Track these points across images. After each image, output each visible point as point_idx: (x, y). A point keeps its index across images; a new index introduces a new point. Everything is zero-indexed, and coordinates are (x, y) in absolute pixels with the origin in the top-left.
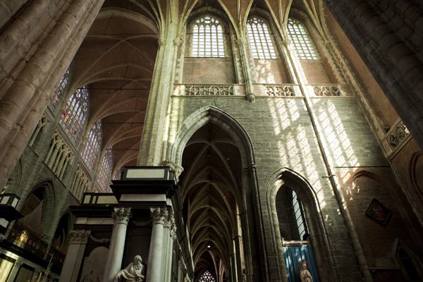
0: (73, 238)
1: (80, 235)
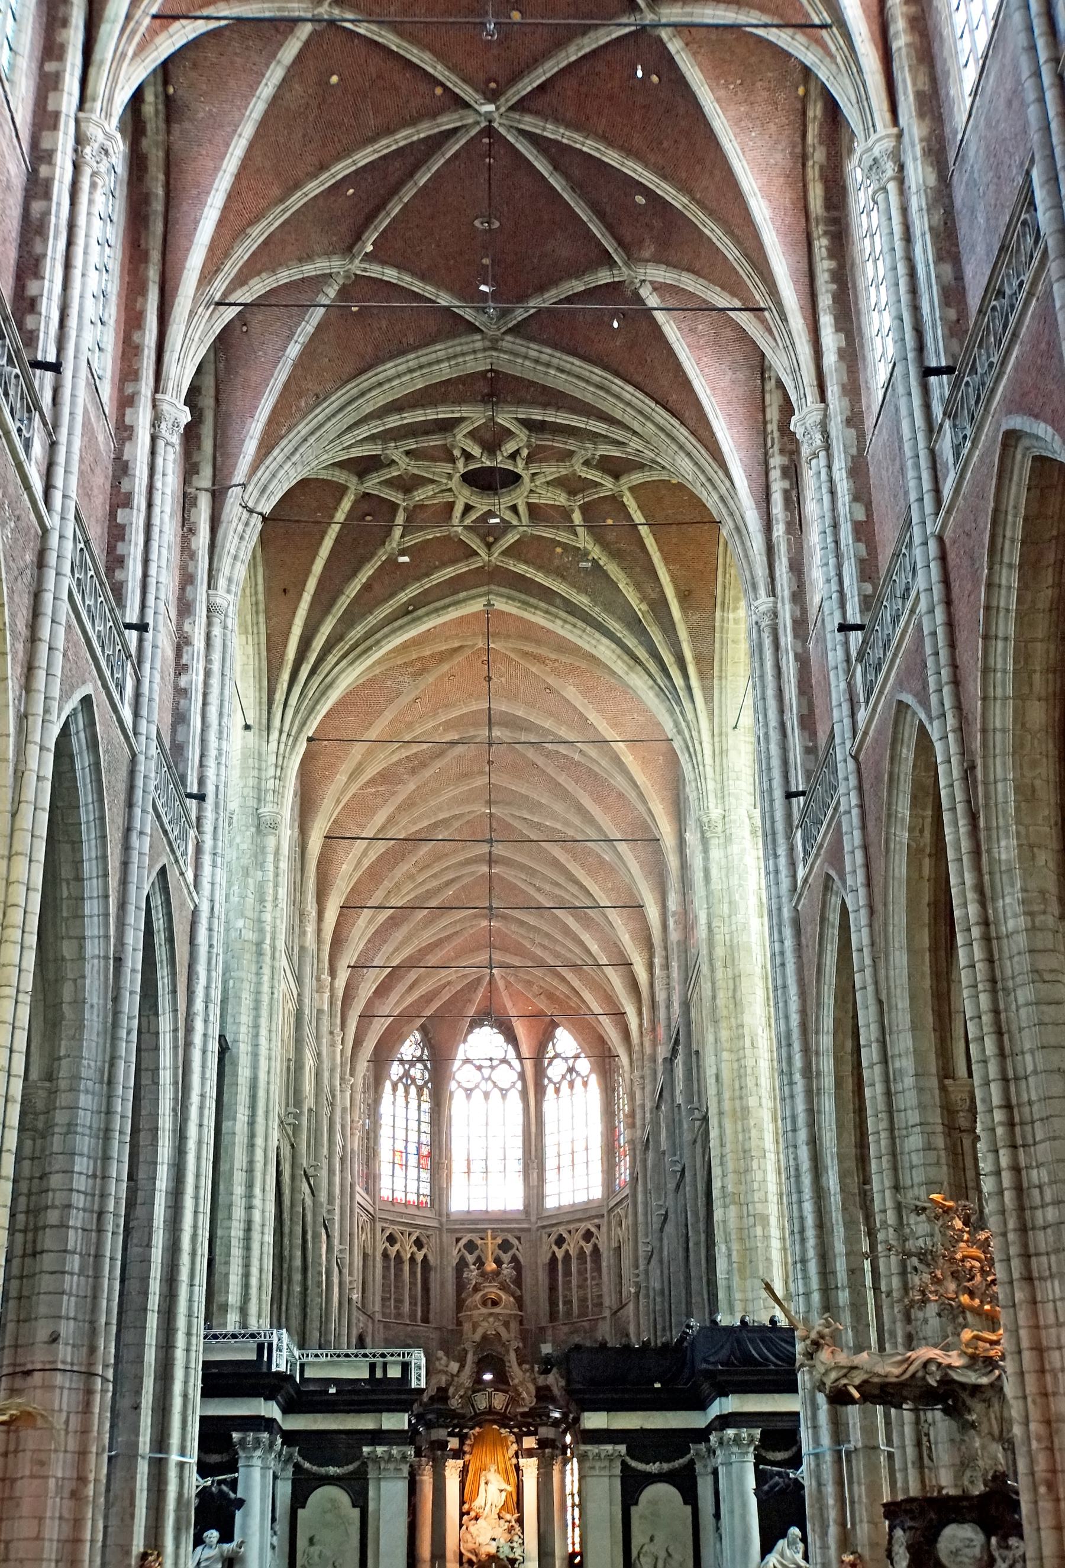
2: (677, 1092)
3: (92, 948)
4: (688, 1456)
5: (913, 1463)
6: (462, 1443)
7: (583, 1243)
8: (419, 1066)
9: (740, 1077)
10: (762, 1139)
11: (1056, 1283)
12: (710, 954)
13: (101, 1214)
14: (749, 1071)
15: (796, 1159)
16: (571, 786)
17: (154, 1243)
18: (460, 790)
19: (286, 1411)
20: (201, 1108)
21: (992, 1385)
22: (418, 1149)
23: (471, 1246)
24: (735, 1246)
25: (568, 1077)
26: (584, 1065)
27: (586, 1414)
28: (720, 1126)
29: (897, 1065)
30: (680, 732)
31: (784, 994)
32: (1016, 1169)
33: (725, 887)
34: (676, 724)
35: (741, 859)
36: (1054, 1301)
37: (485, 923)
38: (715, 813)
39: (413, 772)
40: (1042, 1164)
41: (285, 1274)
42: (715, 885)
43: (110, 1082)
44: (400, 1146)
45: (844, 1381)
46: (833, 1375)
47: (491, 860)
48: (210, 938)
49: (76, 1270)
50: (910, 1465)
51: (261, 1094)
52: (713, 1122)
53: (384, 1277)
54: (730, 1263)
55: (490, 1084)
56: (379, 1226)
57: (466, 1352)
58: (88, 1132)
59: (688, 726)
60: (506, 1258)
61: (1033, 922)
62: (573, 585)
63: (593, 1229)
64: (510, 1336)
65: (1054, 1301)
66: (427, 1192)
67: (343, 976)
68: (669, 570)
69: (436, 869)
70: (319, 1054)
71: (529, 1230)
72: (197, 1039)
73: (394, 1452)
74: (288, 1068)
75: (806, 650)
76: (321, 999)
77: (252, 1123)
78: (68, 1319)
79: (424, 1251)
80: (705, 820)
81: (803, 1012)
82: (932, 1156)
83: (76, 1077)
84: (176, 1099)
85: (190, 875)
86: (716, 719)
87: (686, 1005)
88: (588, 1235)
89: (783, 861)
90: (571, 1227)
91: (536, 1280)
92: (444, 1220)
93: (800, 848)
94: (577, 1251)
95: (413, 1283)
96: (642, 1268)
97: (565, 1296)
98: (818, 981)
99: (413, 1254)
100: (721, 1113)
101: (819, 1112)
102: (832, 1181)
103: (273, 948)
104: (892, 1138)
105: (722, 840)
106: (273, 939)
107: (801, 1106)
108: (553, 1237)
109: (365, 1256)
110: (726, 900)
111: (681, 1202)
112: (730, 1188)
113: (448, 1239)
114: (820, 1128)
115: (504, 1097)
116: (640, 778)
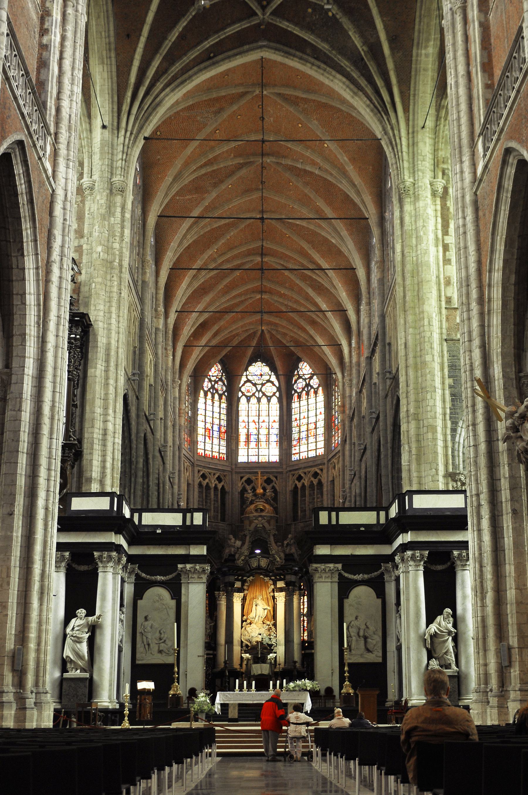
0: (317, 575)
1: (327, 570)
2: (375, 376)
7: (312, 479)
9: (420, 344)
10: (434, 380)
14: (427, 339)
15: (471, 359)
23: (249, 481)
25: (306, 389)
26: (315, 382)
28: (407, 375)
30: (386, 133)
31: (465, 252)
33: (414, 228)
34: (384, 129)
35: (425, 210)
53: (199, 497)
55: (261, 394)
56: (196, 469)
59: (392, 129)
62: (319, 36)
63: (318, 471)
66: (225, 452)
68: (383, 21)
71: (281, 473)
75: (487, 20)
79: (222, 483)
80: (402, 186)
81: (479, 262)
86: (411, 123)
87: (383, 317)
88: (316, 475)
90: (306, 470)
91: (286, 499)
92: (234, 467)
94: (309, 483)
95: (216, 501)
97: (302, 508)
98: (493, 234)
99: (216, 485)
100: (407, 367)
105: (412, 200)
108: (296, 476)
109: (188, 484)
110: (414, 236)
111: (375, 437)
112: (412, 411)
115: (269, 401)
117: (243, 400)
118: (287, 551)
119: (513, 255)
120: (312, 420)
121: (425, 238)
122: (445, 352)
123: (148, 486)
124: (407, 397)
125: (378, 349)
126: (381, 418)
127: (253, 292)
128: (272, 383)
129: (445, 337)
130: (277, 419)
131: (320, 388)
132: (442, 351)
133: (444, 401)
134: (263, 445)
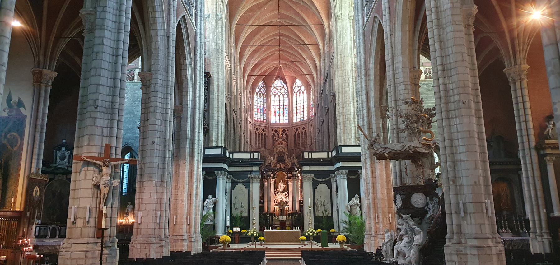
3: (160, 33)
4: (329, 177)
5: (399, 177)
6: (274, 176)
7: (302, 130)
8: (263, 89)
9: (344, 83)
10: (350, 99)
11: (458, 119)
12: (337, 51)
13: (166, 109)
14: (347, 81)
16: (300, 12)
17: (188, 121)
18: (271, 14)
19: (229, 167)
20: (200, 86)
21: (428, 153)
22: (263, 108)
23: (276, 131)
24: (342, 126)
26: (303, 88)
27: (304, 167)
29: (397, 66)
32: (445, 85)
33: (341, 33)
35: (346, 25)
36: (457, 125)
37: (279, 53)
38: (339, 13)
39: (259, 9)
40: (454, 82)
41: (229, 134)
42: (338, 33)
43: (167, 72)
44: (259, 108)
45: (383, 152)
46: (380, 150)
47: (280, 35)
48: (201, 40)
49: (159, 124)
50: (398, 177)
51: (220, 88)
52: (337, 95)
53: (255, 138)
54: (341, 130)
57: (275, 155)
58: (161, 86)
60: (284, 134)
61: (453, 5)
63: (305, 127)
64: (285, 151)
65: (457, 125)
67: (243, 64)
69: (266, 37)
70: (237, 82)
72: (198, 67)
73: (256, 176)
74: (228, 84)
76: (237, 68)
77: (218, 96)
78: (157, 137)
80: (337, 15)
81: (365, 59)
82: (406, 91)
83: (157, 70)
84: (192, 83)
85: (194, 21)
87: (329, 68)
89: (360, 17)
90: (300, 126)
91: (291, 138)
92: (269, 125)
93: (366, 12)
95: (262, 140)
96: (317, 135)
98: (370, 49)
101: (369, 86)
102: (372, 104)
103: (222, 51)
104: (395, 87)
105: (341, 20)
106: (222, 48)
107: (364, 84)
108: (295, 129)
110: (342, 36)
112: (341, 111)
113: (270, 130)
114: (369, 90)
115: (283, 96)
116: (319, 8)
117: (273, 96)
118: (292, 162)
119: (378, 57)
120: (302, 104)
121: (346, 37)
122: (354, 86)
123: (235, 139)
124: (339, 105)
125: (328, 80)
126: (329, 111)
127: (276, 51)
128: (285, 88)
129: (354, 80)
130: (287, 104)
131: (305, 91)
132: (353, 86)
133: (354, 107)
134: (281, 115)
